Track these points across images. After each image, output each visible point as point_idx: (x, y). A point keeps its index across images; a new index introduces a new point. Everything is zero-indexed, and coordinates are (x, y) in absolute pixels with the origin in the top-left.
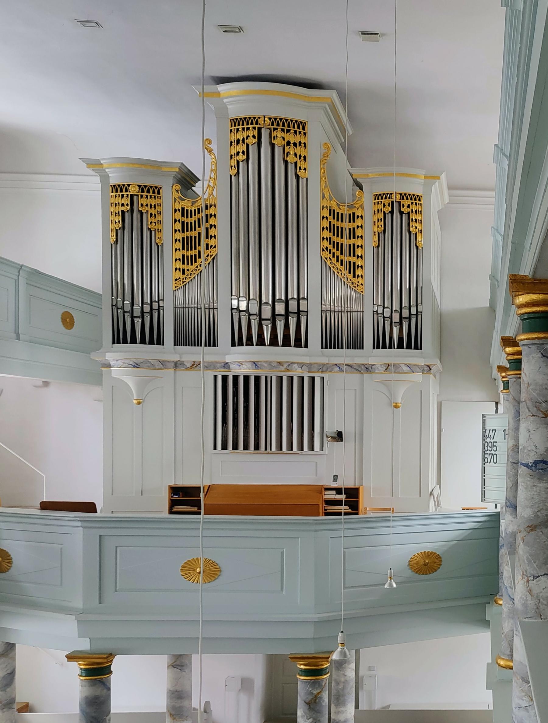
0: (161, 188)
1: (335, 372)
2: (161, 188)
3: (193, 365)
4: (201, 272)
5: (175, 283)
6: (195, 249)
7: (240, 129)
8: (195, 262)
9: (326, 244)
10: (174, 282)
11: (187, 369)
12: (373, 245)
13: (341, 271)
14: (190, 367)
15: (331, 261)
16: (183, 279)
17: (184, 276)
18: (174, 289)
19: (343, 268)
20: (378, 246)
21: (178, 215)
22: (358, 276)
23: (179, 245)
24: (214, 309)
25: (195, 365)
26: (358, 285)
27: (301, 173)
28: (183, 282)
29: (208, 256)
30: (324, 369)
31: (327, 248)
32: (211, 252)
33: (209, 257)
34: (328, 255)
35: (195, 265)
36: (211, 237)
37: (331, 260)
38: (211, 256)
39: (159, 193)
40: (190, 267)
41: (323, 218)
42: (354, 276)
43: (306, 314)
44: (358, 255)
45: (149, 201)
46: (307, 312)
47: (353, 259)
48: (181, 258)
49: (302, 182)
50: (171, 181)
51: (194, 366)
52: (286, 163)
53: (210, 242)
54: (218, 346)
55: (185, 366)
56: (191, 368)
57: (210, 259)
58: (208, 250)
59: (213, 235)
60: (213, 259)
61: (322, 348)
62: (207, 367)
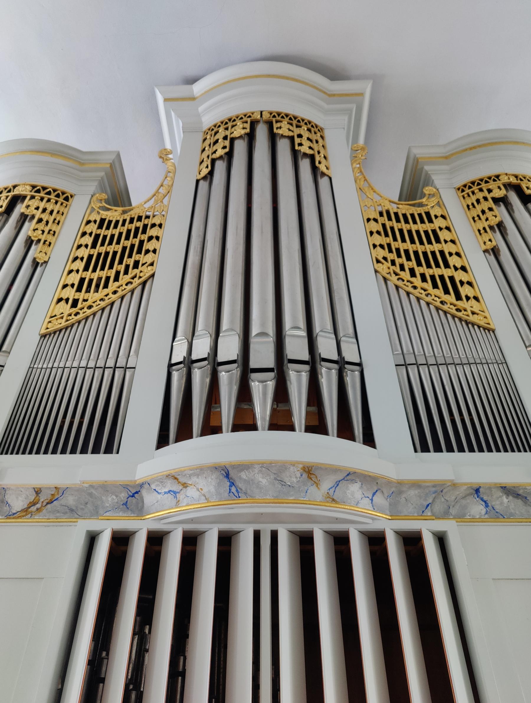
0: (72, 196)
1: (473, 520)
2: (72, 196)
3: (33, 504)
4: (112, 304)
5: (50, 322)
6: (111, 267)
7: (220, 131)
8: (106, 286)
9: (381, 253)
10: (48, 320)
11: (12, 516)
12: (484, 247)
13: (425, 290)
14: (22, 511)
15: (398, 277)
16: (70, 315)
17: (74, 310)
18: (43, 331)
19: (429, 286)
20: (495, 252)
21: (93, 228)
22: (468, 298)
23: (80, 265)
24: (126, 368)
25: (38, 506)
26: (473, 313)
27: (322, 168)
28: (67, 320)
29: (133, 278)
30: (438, 507)
31: (385, 259)
32: (141, 272)
33: (136, 279)
34: (389, 268)
35: (102, 292)
36: (147, 251)
37: (396, 274)
38: (140, 277)
39: (67, 199)
40: (93, 296)
41: (369, 220)
42: (458, 297)
43: (357, 368)
44: (454, 266)
45: (42, 205)
46: (360, 365)
47: (447, 273)
48: (76, 284)
49: (323, 182)
50: (92, 187)
51: (33, 509)
52: (295, 154)
53: (143, 257)
54: (118, 453)
55: (6, 508)
56: (24, 514)
57: (137, 281)
58: (138, 268)
59: (151, 249)
60: (144, 284)
61: (416, 451)
62: (72, 510)
